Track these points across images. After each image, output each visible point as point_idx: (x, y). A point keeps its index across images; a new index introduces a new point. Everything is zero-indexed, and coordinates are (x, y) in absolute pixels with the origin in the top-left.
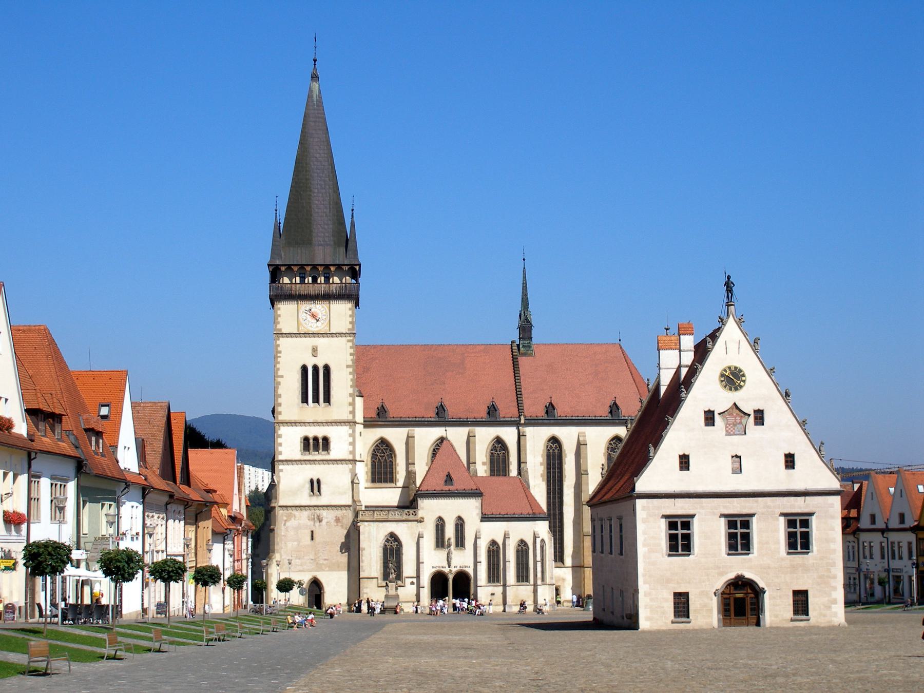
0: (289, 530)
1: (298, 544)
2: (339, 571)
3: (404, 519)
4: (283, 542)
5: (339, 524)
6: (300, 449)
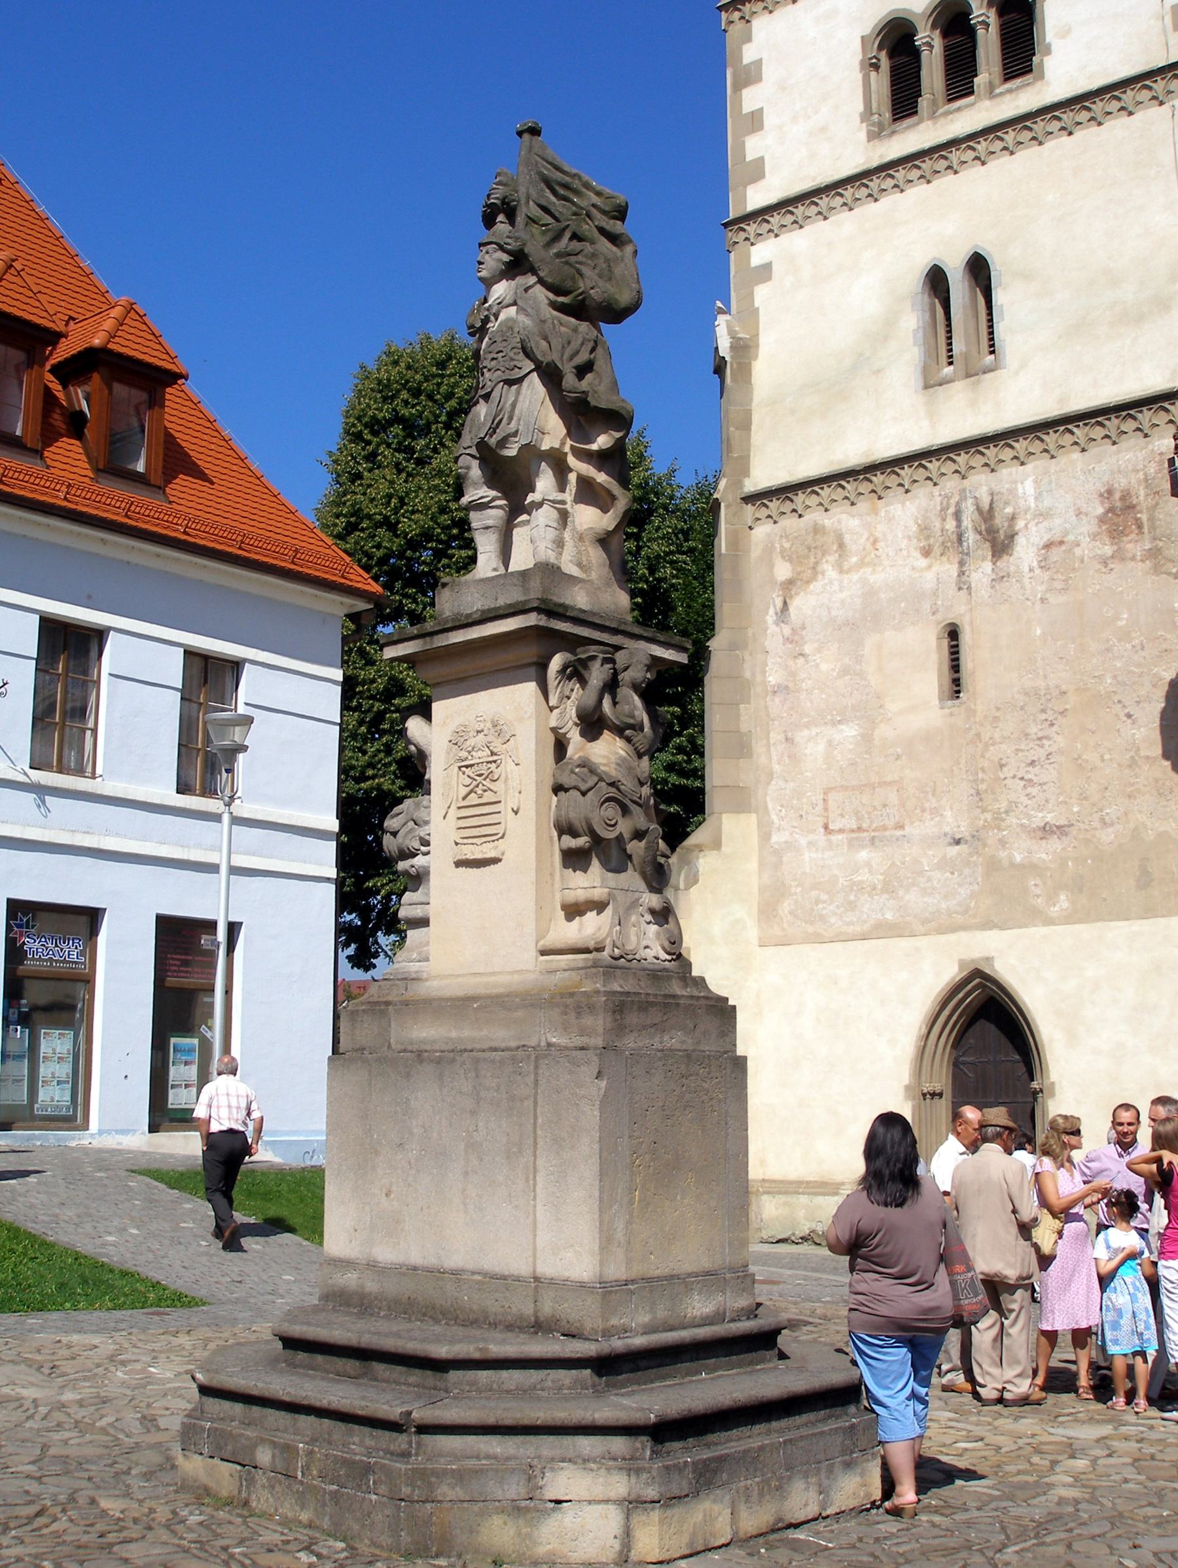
0: (807, 649)
1: (866, 739)
2: (1149, 912)
4: (774, 736)
5: (1136, 546)
6: (860, 107)
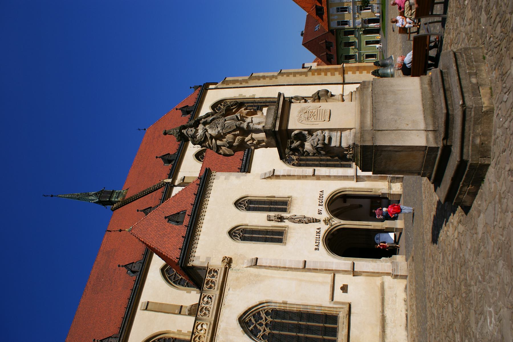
3: (218, 293)
